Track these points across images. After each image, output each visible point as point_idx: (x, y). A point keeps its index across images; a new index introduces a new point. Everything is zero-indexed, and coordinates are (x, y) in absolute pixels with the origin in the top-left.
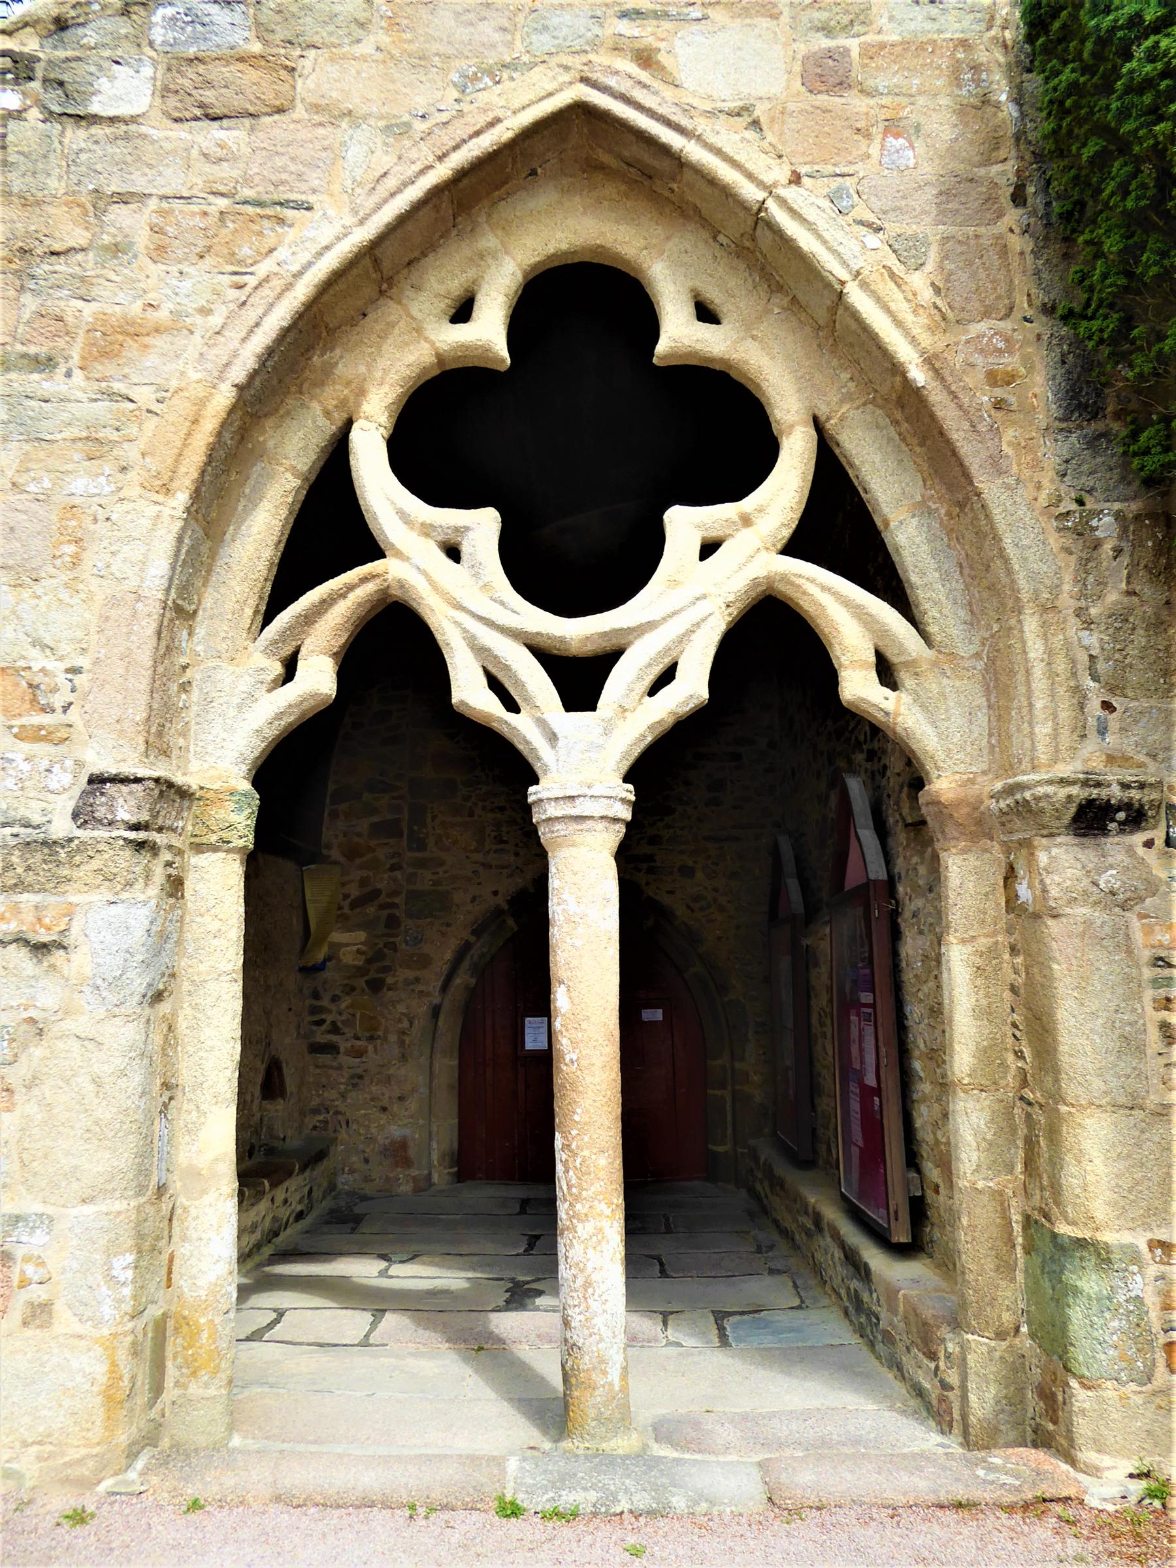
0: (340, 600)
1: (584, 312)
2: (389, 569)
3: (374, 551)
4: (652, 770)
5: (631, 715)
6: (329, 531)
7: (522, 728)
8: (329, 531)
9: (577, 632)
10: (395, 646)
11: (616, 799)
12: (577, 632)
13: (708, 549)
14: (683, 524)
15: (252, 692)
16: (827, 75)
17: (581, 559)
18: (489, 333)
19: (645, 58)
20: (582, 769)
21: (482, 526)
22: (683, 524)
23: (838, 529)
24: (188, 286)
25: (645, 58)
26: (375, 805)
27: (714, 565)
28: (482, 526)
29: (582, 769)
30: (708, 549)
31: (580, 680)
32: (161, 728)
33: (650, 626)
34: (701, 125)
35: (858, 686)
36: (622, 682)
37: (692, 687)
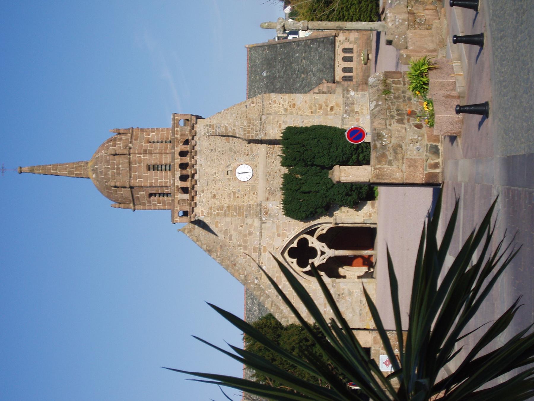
4: (330, 247)
5: (326, 249)
7: (327, 258)
14: (310, 245)
16: (279, 235)
18: (295, 260)
19: (277, 249)
20: (331, 253)
22: (310, 245)
23: (311, 232)
25: (277, 249)
27: (313, 242)
29: (331, 253)
31: (323, 253)
36: (323, 250)
37: (324, 244)
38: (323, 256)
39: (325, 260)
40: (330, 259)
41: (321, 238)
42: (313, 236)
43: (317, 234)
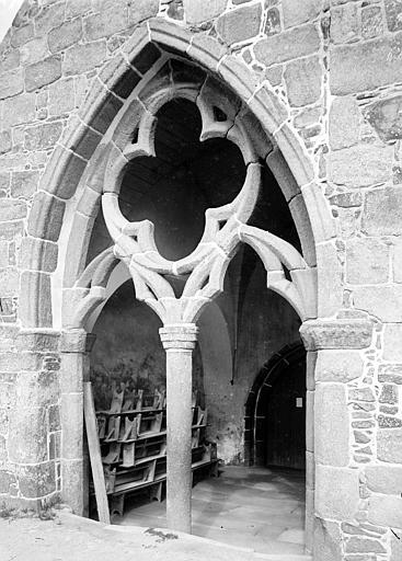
0: (102, 261)
2: (115, 249)
3: (111, 242)
5: (196, 297)
6: (98, 236)
8: (98, 236)
9: (174, 267)
12: (174, 267)
15: (73, 303)
17: (181, 234)
18: (145, 146)
20: (178, 322)
21: (144, 227)
24: (34, 157)
27: (228, 225)
29: (178, 322)
30: (222, 224)
32: (43, 315)
34: (192, 38)
35: (275, 281)
37: (217, 284)
38: (162, 286)
39: (149, 300)
41: (245, 264)
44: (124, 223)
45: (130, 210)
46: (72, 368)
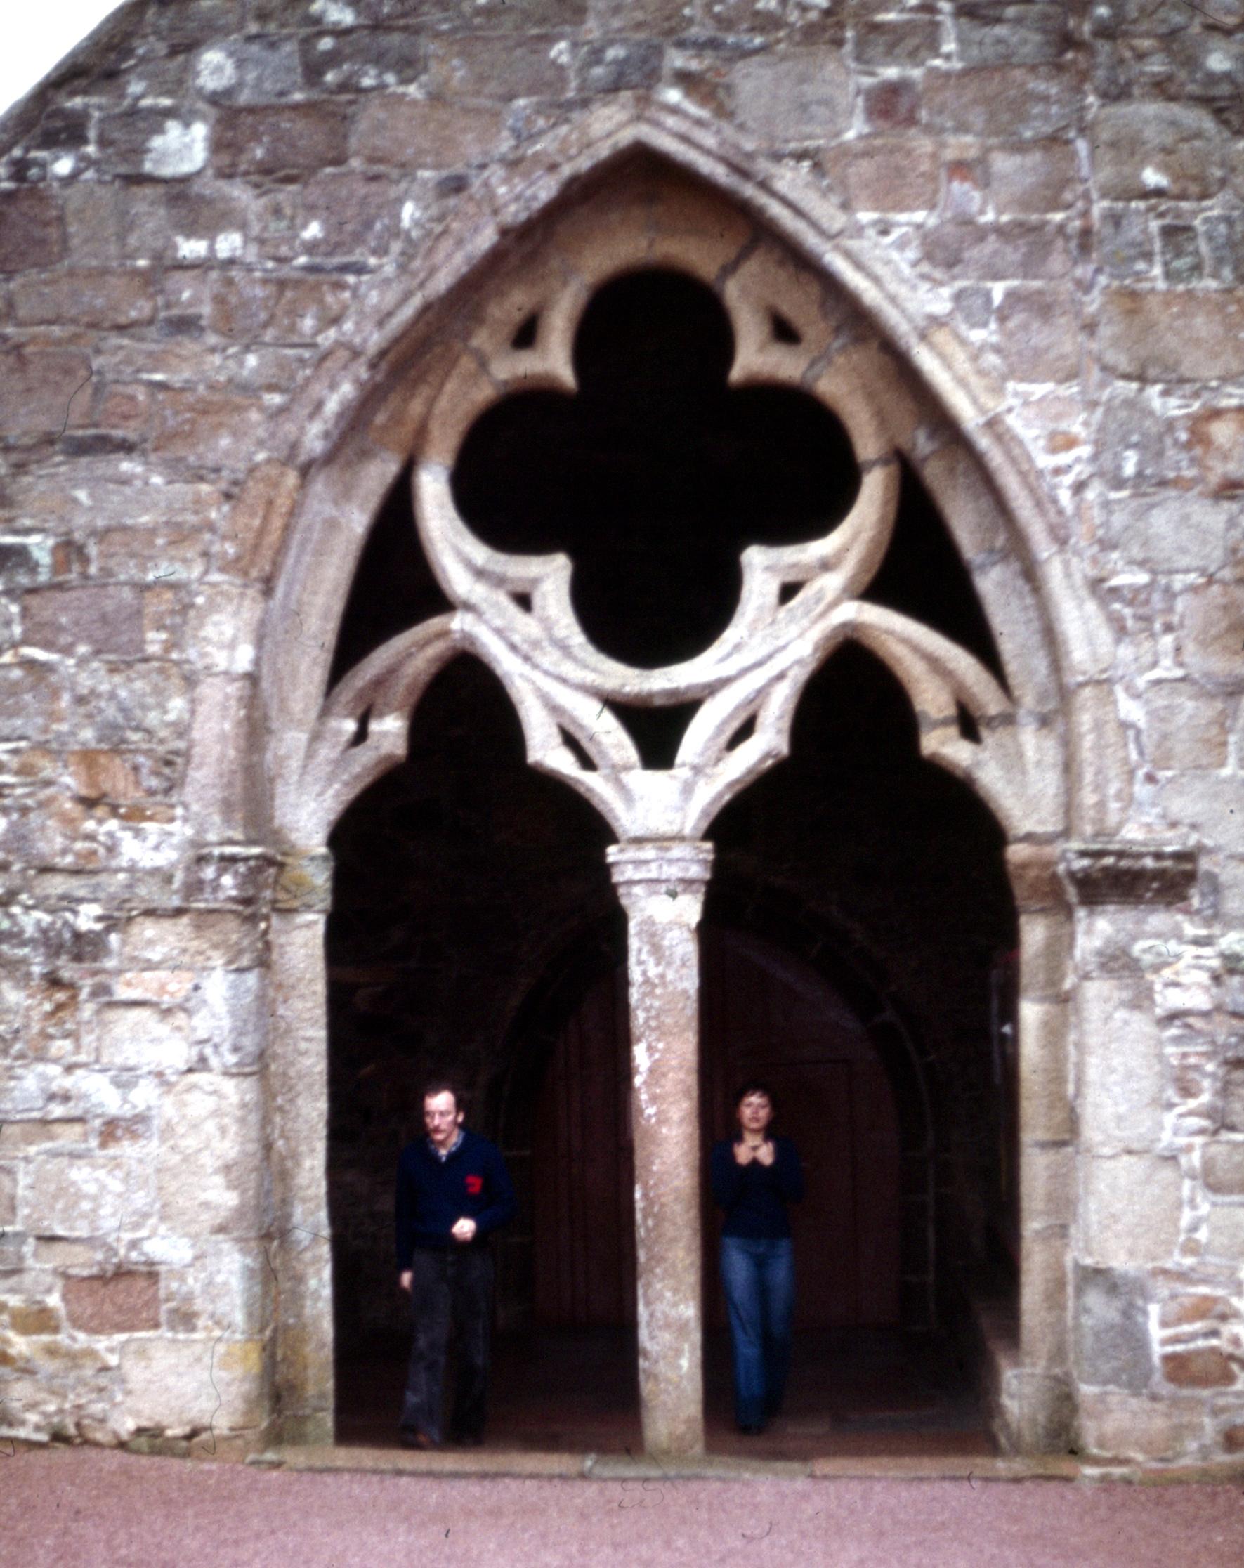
0: (411, 653)
1: (656, 325)
4: (733, 826)
5: (709, 771)
6: (392, 584)
7: (595, 784)
8: (392, 584)
10: (468, 702)
11: (694, 862)
13: (788, 592)
14: (761, 566)
17: (654, 604)
18: (555, 361)
20: (660, 831)
21: (552, 575)
22: (761, 566)
26: (450, 898)
28: (552, 575)
29: (660, 831)
30: (788, 592)
31: (657, 731)
33: (712, 689)
36: (698, 737)
37: (770, 740)
39: (561, 762)
40: (583, 829)
42: (879, 589)
43: (901, 635)
44: (480, 553)
45: (498, 515)
46: (304, 942)
